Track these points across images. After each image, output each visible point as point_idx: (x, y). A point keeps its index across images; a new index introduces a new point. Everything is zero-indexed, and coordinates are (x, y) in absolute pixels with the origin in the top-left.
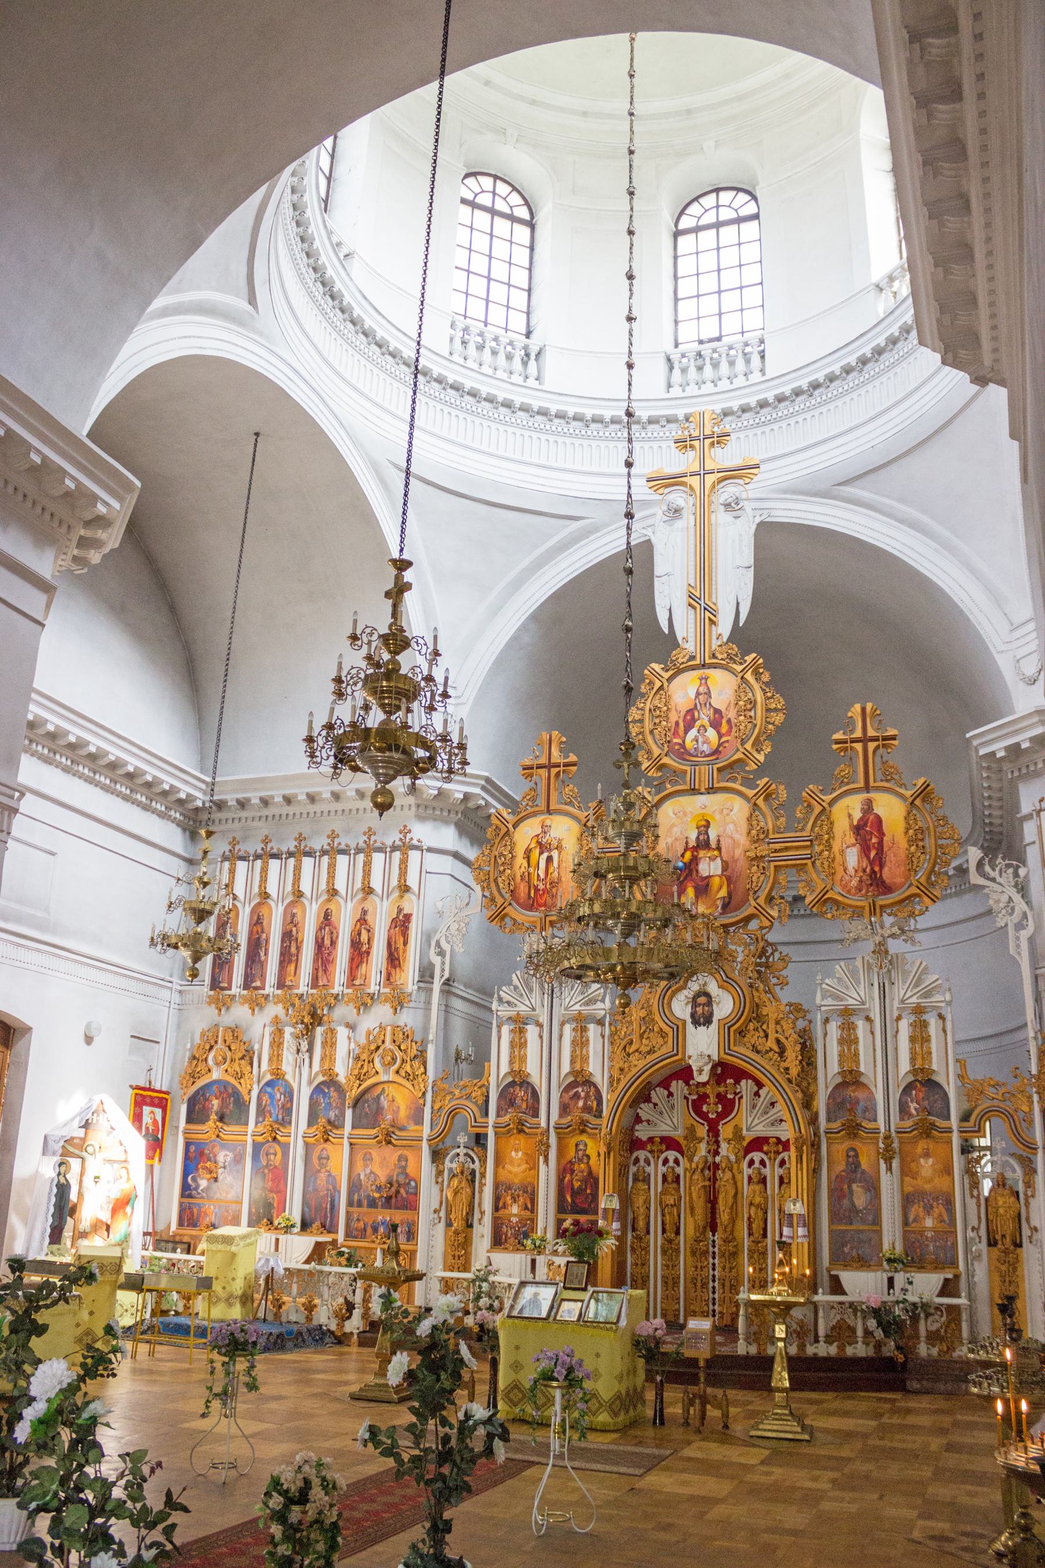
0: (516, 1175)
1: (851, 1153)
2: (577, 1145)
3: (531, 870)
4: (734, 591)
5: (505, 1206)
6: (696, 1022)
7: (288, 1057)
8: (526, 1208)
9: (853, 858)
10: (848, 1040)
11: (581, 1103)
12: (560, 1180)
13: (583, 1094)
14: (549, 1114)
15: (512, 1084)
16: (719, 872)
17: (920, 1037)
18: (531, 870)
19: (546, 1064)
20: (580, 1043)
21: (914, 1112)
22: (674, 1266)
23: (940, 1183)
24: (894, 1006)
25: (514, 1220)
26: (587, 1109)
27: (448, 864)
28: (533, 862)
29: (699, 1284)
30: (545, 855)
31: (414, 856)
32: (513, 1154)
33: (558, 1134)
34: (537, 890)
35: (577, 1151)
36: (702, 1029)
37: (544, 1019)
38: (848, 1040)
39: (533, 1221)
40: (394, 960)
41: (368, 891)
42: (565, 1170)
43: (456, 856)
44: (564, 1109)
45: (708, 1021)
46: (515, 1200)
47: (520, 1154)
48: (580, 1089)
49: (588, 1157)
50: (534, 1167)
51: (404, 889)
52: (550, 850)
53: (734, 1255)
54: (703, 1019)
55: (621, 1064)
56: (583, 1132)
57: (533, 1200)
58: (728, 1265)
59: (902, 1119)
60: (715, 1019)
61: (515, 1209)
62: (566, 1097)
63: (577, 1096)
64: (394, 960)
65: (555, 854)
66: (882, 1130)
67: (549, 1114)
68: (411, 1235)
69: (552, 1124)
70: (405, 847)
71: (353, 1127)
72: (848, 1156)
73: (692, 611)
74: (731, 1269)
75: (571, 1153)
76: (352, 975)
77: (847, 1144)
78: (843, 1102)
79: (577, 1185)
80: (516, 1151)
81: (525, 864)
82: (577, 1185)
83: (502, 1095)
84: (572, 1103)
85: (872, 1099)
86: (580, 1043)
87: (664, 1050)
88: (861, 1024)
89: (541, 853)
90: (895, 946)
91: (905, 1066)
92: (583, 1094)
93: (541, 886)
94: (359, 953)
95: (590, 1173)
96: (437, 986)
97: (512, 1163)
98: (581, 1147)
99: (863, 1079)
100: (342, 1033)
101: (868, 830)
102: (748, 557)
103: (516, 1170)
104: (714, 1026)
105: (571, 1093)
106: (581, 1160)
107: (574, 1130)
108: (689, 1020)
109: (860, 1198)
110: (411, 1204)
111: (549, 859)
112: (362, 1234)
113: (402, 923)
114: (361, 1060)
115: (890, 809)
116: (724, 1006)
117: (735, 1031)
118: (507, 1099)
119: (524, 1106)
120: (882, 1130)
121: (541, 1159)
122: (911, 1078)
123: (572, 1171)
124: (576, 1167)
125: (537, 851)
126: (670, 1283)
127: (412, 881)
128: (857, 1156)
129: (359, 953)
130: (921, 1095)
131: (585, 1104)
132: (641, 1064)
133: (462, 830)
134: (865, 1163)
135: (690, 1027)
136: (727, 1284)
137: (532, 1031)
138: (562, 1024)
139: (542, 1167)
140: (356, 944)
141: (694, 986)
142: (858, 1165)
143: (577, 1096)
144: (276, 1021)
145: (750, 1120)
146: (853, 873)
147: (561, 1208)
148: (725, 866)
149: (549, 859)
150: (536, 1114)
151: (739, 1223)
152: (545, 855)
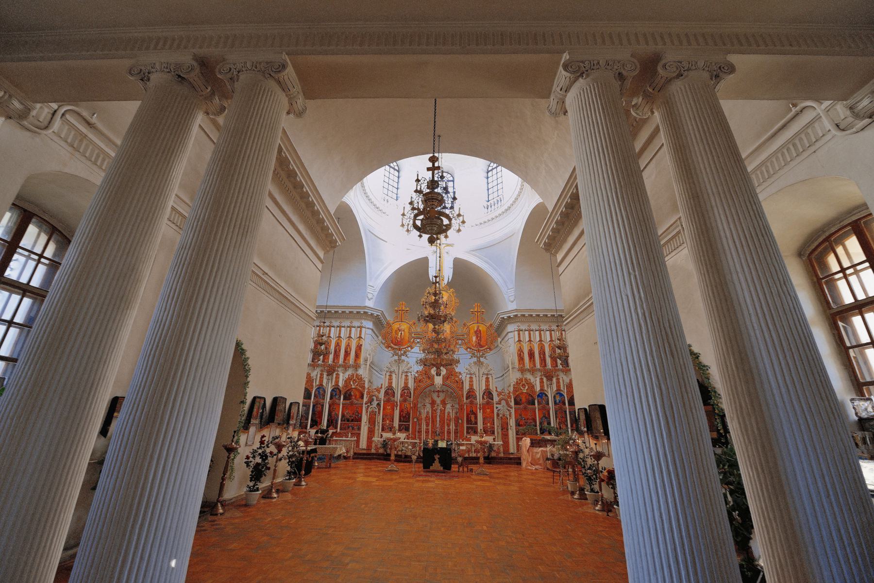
4: (448, 273)
7: (325, 381)
9: (474, 339)
10: (471, 381)
14: (398, 397)
17: (487, 380)
19: (398, 385)
20: (406, 379)
24: (481, 373)
27: (370, 332)
31: (363, 330)
38: (471, 381)
40: (357, 356)
41: (350, 337)
42: (401, 411)
51: (360, 337)
54: (438, 374)
64: (357, 356)
67: (398, 397)
68: (359, 429)
70: (361, 327)
71: (344, 399)
76: (345, 359)
86: (406, 379)
88: (474, 376)
90: (482, 359)
91: (484, 388)
94: (347, 354)
96: (368, 363)
100: (341, 375)
101: (478, 333)
102: (452, 266)
109: (473, 417)
110: (360, 420)
112: (345, 429)
113: (359, 347)
114: (347, 382)
115: (482, 328)
117: (446, 378)
118: (386, 393)
127: (363, 336)
129: (347, 354)
133: (374, 323)
137: (394, 376)
140: (346, 352)
144: (322, 371)
147: (400, 421)
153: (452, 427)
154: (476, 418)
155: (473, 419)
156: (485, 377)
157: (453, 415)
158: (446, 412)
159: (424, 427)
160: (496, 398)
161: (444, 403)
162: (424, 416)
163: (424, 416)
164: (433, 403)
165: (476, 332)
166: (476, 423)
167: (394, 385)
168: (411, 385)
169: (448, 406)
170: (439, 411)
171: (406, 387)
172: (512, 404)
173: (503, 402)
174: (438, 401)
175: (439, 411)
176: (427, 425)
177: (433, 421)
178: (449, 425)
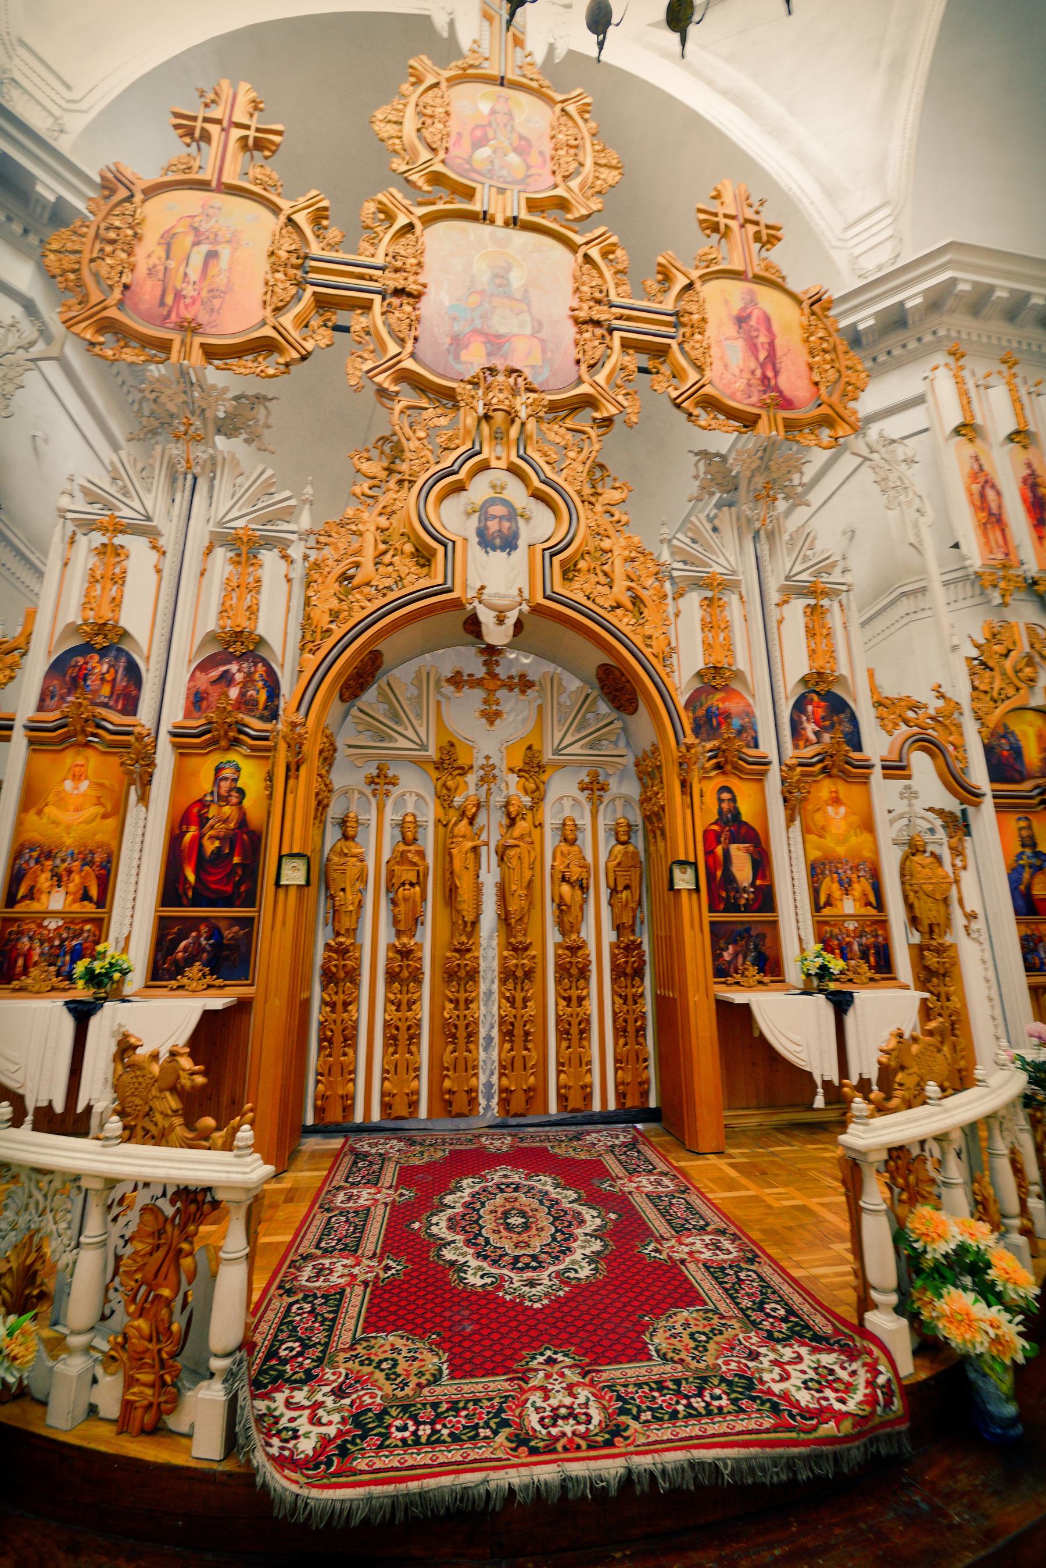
0: (68, 828)
1: (726, 796)
2: (218, 770)
3: (171, 264)
5: (31, 895)
6: (486, 542)
8: (86, 897)
11: (234, 693)
12: (174, 840)
13: (239, 677)
15: (86, 649)
16: (528, 331)
18: (171, 264)
21: (813, 737)
22: (411, 1004)
23: (859, 840)
25: (53, 924)
26: (245, 703)
28: (177, 251)
29: (462, 1034)
30: (204, 248)
32: (68, 785)
33: (176, 746)
34: (178, 295)
35: (217, 779)
36: (498, 556)
37: (167, 541)
39: (101, 924)
42: (189, 816)
43: (29, 307)
44: (197, 700)
45: (509, 544)
46: (58, 879)
47: (84, 785)
48: (234, 667)
49: (242, 793)
50: (118, 811)
52: (215, 242)
53: (528, 974)
54: (500, 540)
55: (334, 603)
56: (235, 742)
57: (106, 879)
58: (519, 996)
59: (796, 747)
60: (522, 543)
61: (57, 901)
62: (203, 681)
63: (226, 679)
65: (225, 252)
66: (774, 757)
69: (165, 727)
72: (720, 801)
73: (486, 24)
74: (525, 1000)
75: (204, 783)
77: (720, 781)
78: (709, 715)
79: (210, 846)
80: (77, 778)
81: (161, 252)
82: (210, 846)
83: (58, 667)
84: (214, 692)
85: (749, 714)
87: (423, 583)
89: (196, 243)
91: (796, 665)
92: (239, 677)
93: (189, 291)
95: (243, 821)
97: (62, 801)
98: (227, 773)
99: (735, 685)
103: (67, 817)
104: (521, 553)
105: (215, 673)
106: (224, 799)
107: (215, 741)
108: (474, 540)
111: (212, 255)
116: (540, 526)
118: (68, 673)
119: (106, 690)
120: (774, 757)
121: (133, 797)
122: (802, 690)
123: (202, 821)
124: (212, 811)
125: (190, 239)
126: (403, 1036)
128: (733, 800)
130: (821, 712)
131: (242, 694)
132: (371, 607)
134: (747, 811)
135: (475, 550)
136: (518, 1032)
137: (138, 551)
138: (209, 550)
139: (134, 812)
141: (479, 490)
142: (736, 814)
143: (226, 679)
145: (558, 736)
146: (737, 372)
147: (171, 891)
148: (538, 326)
149: (212, 255)
150: (130, 706)
151: (536, 914)
152: (204, 248)
153: (598, 933)
154: (762, 863)
155: (743, 870)
156: (798, 605)
157: (599, 850)
158: (550, 817)
159: (375, 937)
160: (876, 744)
161: (532, 767)
162: (376, 847)
163: (376, 847)
164: (448, 763)
165: (741, 320)
166: (765, 898)
167: (136, 618)
168: (276, 624)
169: (563, 794)
170: (492, 828)
171: (236, 648)
172: (979, 775)
173: (921, 762)
174: (490, 744)
175: (492, 828)
176: (406, 924)
177: (450, 894)
178: (567, 924)
